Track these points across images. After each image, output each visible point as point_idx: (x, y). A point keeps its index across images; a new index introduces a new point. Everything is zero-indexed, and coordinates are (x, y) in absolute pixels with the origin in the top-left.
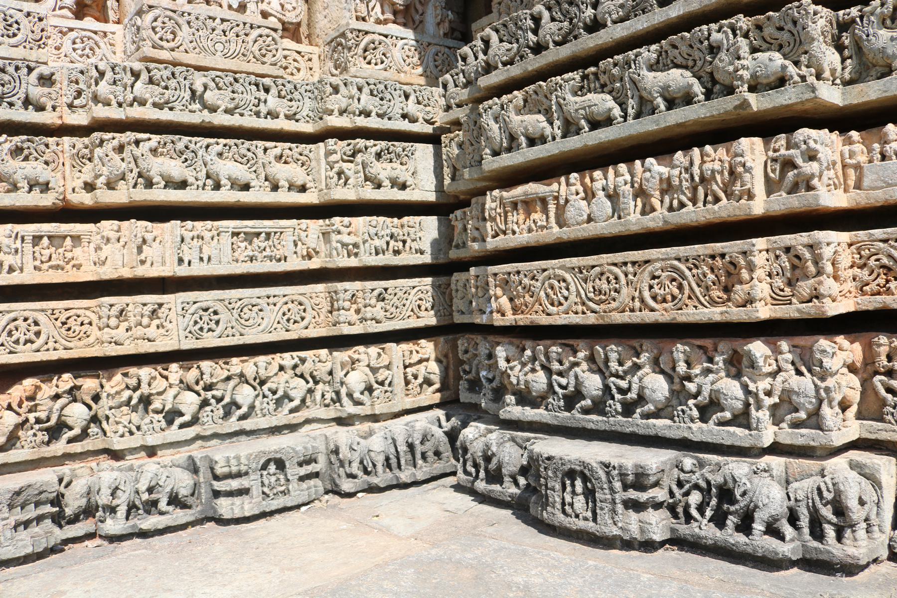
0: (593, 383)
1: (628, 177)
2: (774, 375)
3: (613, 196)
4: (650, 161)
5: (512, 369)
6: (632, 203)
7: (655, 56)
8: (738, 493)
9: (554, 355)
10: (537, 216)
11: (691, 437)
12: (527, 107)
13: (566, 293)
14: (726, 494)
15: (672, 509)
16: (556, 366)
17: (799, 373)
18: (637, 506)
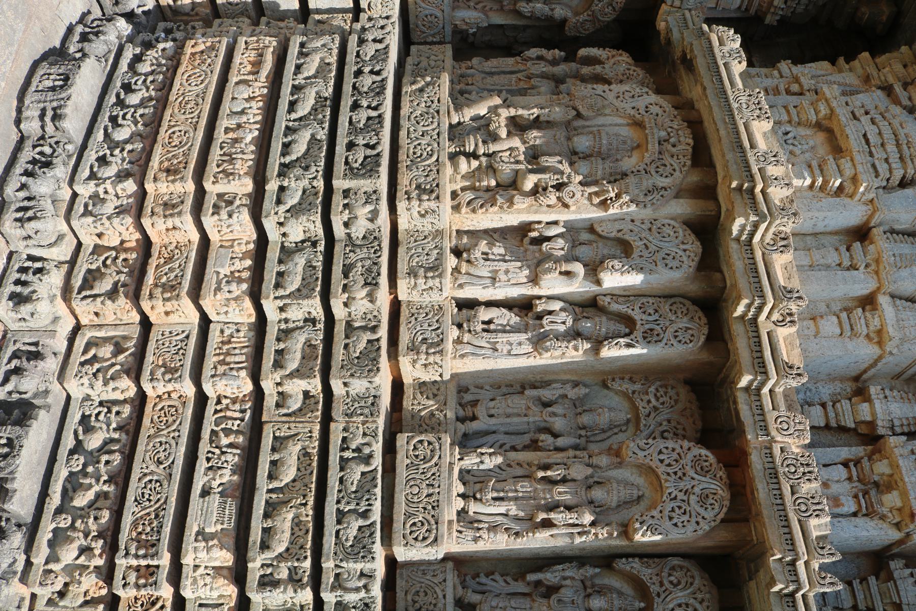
0: (133, 100)
1: (252, 121)
2: (117, 196)
3: (243, 112)
4: (256, 133)
5: (157, 52)
6: (234, 122)
7: (319, 138)
8: (45, 170)
9: (157, 77)
10: (249, 68)
11: (87, 151)
12: (324, 67)
13: (193, 84)
14: (48, 165)
15: (42, 138)
16: (150, 78)
17: (116, 208)
18: (42, 116)
